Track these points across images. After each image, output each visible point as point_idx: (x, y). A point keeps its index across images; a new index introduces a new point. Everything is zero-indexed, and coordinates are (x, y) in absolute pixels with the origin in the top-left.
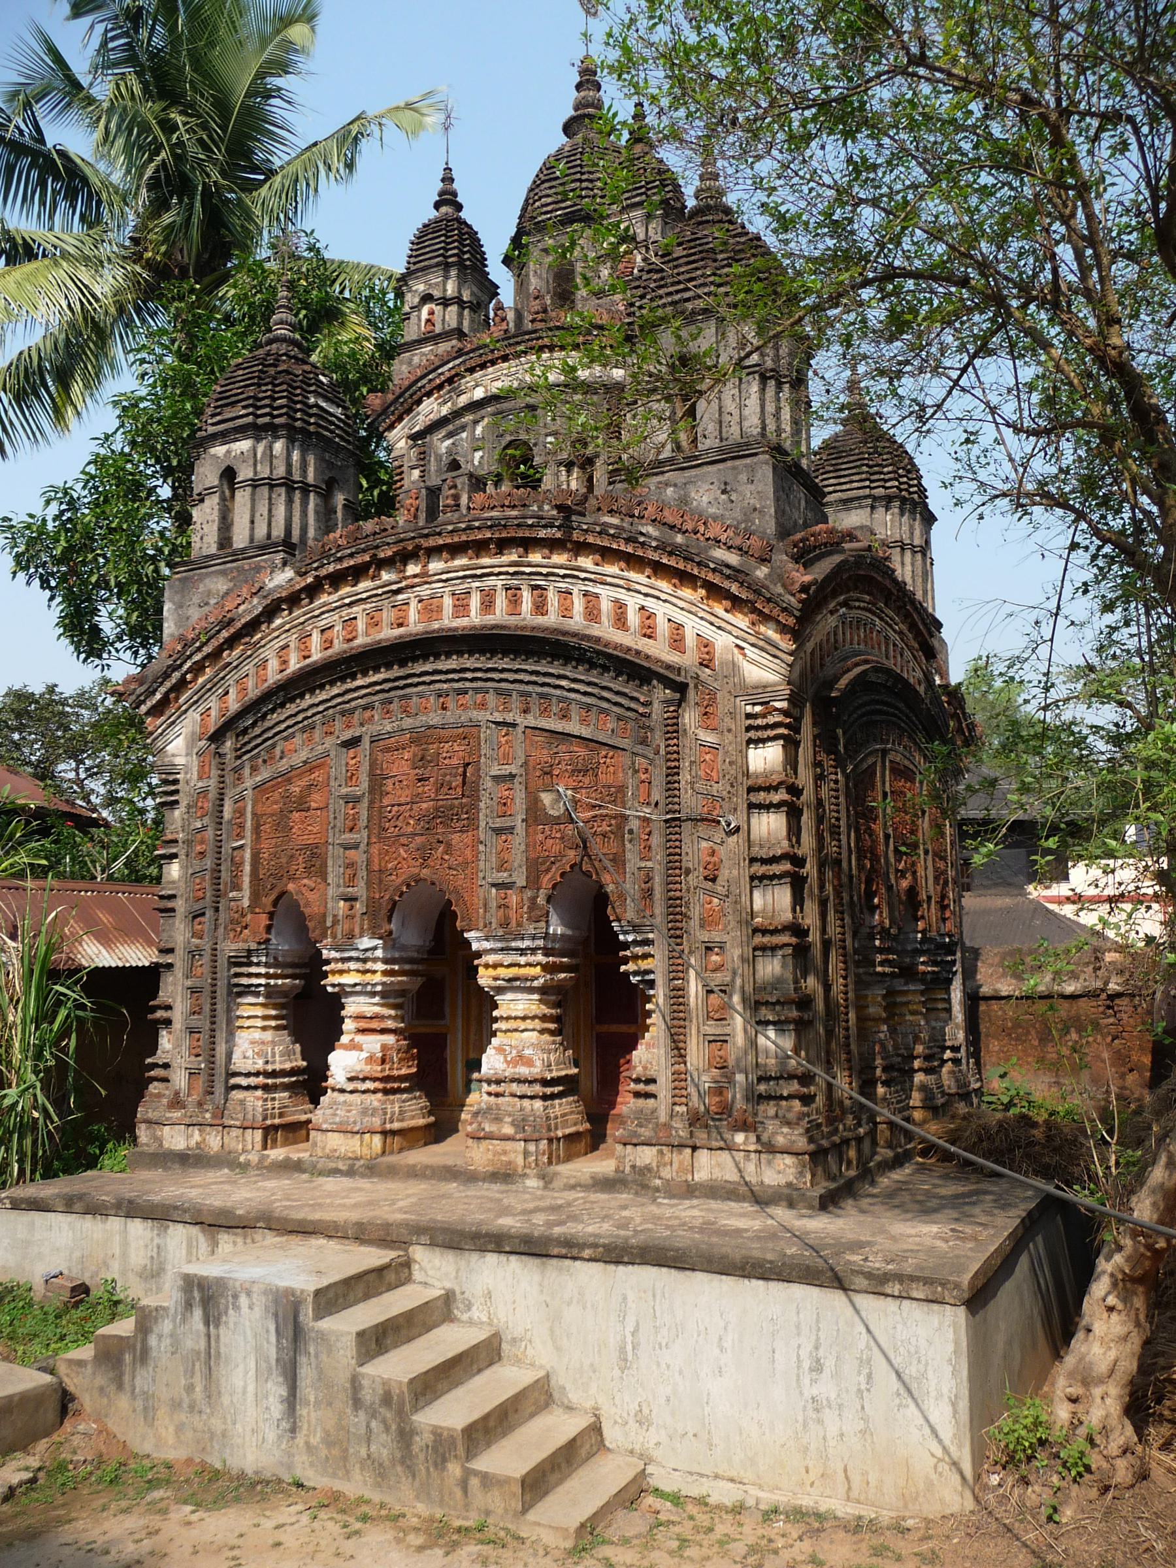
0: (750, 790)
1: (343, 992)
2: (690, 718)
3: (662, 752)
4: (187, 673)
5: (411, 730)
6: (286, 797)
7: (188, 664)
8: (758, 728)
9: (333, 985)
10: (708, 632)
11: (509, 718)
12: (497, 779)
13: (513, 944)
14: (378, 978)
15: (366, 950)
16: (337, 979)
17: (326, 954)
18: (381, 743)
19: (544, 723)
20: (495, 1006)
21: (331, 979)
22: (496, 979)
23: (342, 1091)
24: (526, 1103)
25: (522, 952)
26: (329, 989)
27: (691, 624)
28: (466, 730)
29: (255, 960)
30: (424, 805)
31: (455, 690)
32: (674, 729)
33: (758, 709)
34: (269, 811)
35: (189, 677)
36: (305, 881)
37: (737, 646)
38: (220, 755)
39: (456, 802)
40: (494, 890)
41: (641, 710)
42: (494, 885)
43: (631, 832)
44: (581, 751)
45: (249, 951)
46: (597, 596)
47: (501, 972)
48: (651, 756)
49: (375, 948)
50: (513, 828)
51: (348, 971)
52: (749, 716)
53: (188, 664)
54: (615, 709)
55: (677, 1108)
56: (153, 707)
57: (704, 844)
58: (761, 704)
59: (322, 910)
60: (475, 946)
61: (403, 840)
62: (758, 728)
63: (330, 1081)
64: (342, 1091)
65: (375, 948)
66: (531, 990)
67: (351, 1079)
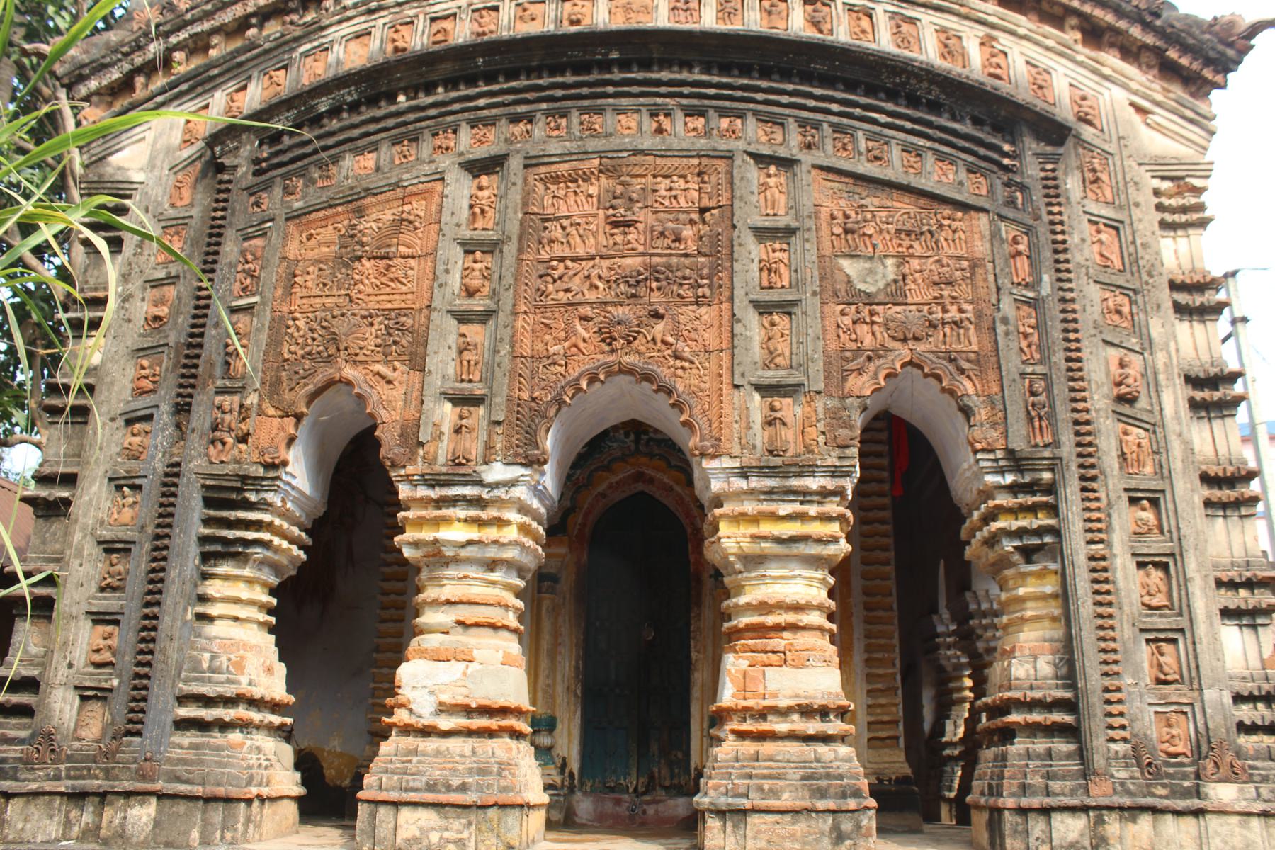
0: (1174, 286)
1: (438, 556)
2: (1072, 184)
3: (1046, 218)
4: (177, 47)
5: (600, 154)
6: (351, 235)
7: (183, 35)
8: (1173, 210)
9: (416, 544)
10: (1088, 82)
11: (782, 152)
12: (762, 233)
13: (795, 483)
14: (511, 533)
15: (496, 485)
16: (427, 535)
17: (404, 491)
18: (543, 169)
19: (846, 166)
20: (740, 590)
21: (410, 535)
22: (755, 538)
23: (427, 732)
24: (822, 749)
25: (804, 495)
26: (407, 552)
27: (1061, 70)
28: (705, 161)
29: (253, 497)
30: (629, 261)
31: (683, 107)
32: (1053, 192)
33: (1166, 185)
34: (310, 255)
35: (178, 56)
36: (378, 367)
37: (1132, 104)
38: (221, 168)
39: (687, 261)
40: (757, 396)
41: (1006, 161)
42: (758, 388)
43: (1005, 321)
44: (904, 207)
45: (244, 478)
46: (912, 21)
47: (767, 528)
48: (1031, 222)
49: (513, 483)
50: (794, 303)
51: (447, 521)
52: (1157, 193)
53: (183, 35)
54: (963, 156)
55: (1113, 746)
56: (98, 92)
57: (1114, 354)
58: (1172, 179)
59: (412, 414)
60: (716, 486)
61: (586, 311)
62: (1173, 210)
63: (401, 716)
64: (427, 732)
65: (513, 483)
66: (814, 562)
67: (445, 709)
